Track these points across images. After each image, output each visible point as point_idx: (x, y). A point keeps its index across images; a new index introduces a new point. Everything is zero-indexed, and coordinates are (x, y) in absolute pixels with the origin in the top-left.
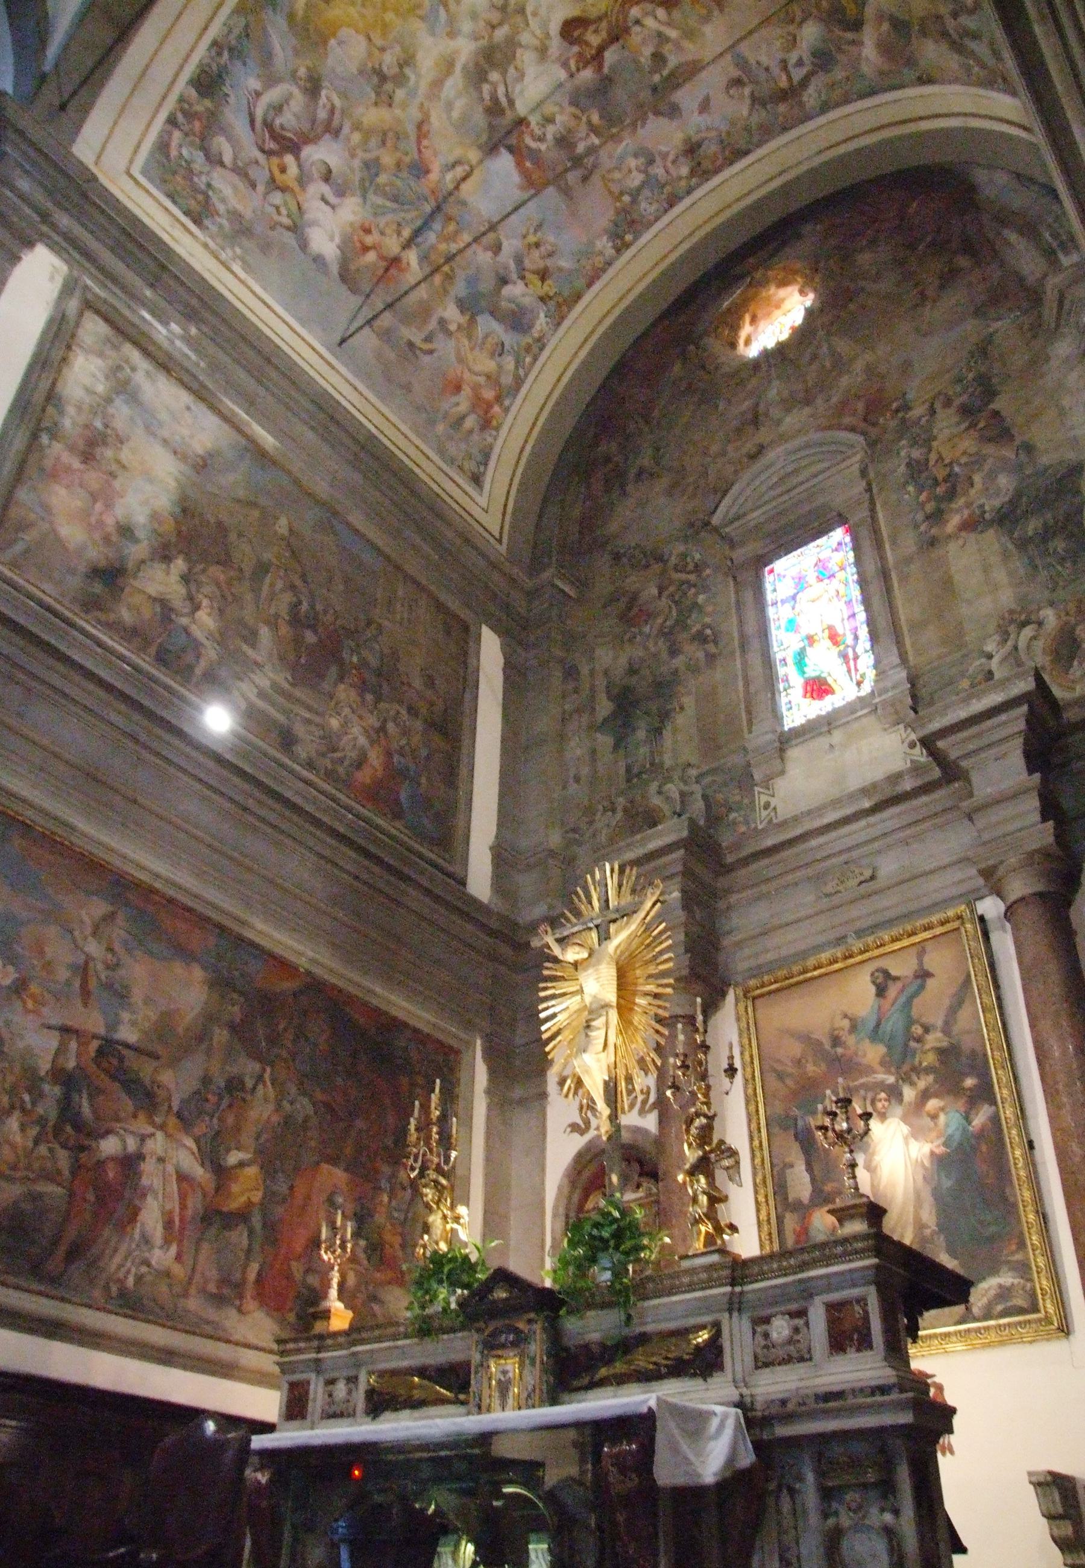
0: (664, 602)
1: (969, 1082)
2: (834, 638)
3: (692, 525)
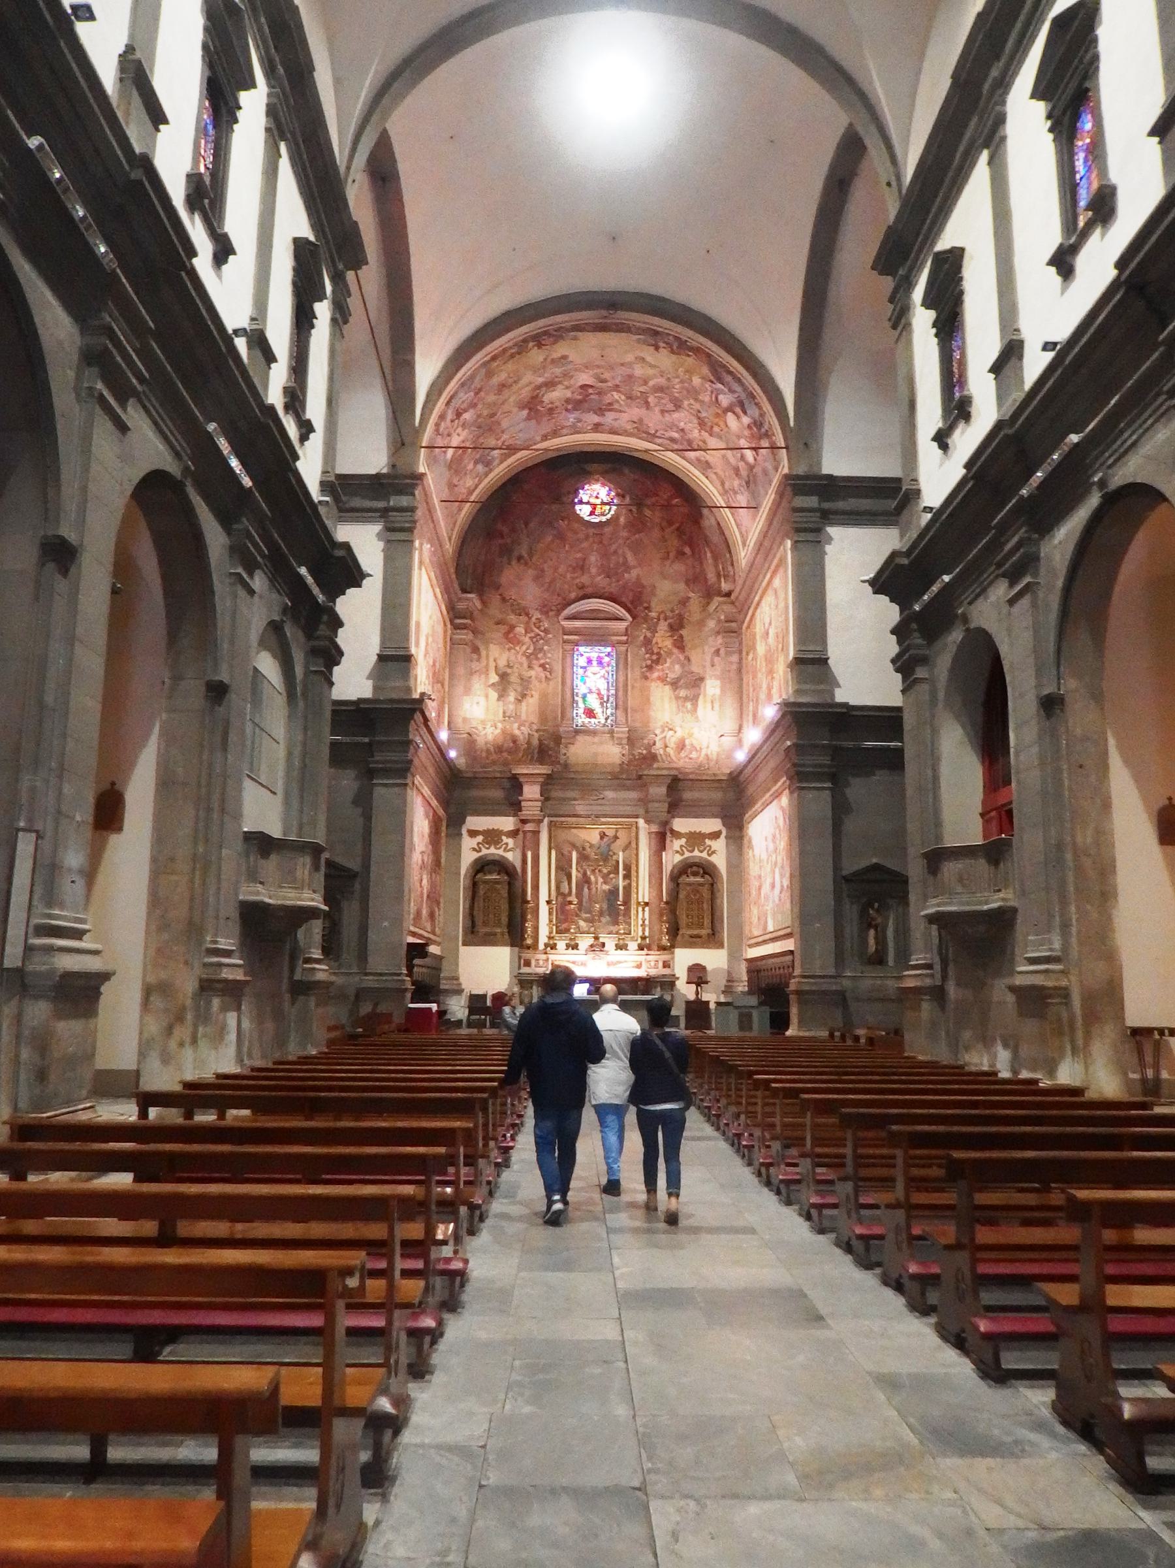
0: (527, 639)
2: (599, 694)
3: (545, 606)
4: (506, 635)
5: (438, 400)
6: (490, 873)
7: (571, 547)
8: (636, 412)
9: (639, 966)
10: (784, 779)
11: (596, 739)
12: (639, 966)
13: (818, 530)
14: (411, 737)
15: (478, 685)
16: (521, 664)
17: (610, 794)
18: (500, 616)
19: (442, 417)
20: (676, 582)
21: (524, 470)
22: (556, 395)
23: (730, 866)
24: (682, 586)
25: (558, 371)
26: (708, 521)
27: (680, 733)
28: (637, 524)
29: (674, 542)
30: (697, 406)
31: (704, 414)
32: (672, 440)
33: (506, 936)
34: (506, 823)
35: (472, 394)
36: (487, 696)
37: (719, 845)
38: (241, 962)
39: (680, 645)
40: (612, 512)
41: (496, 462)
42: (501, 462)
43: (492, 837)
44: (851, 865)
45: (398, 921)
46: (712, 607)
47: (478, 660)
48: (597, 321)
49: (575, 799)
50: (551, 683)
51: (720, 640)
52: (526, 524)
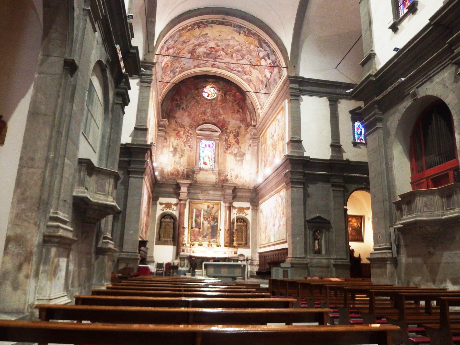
0: (184, 136)
1: (216, 220)
2: (209, 158)
3: (191, 125)
4: (177, 134)
5: (162, 39)
6: (167, 218)
7: (201, 106)
8: (228, 60)
9: (225, 253)
10: (284, 184)
11: (207, 173)
12: (225, 253)
13: (299, 96)
14: (146, 159)
15: (166, 151)
16: (182, 145)
17: (211, 192)
18: (175, 128)
19: (162, 47)
20: (237, 120)
21: (186, 79)
22: (201, 50)
23: (253, 219)
24: (238, 122)
25: (203, 40)
26: (248, 101)
27: (236, 172)
28: (224, 100)
29: (236, 108)
30: (251, 57)
31: (253, 61)
32: (239, 71)
33: (172, 242)
34: (174, 201)
35: (173, 42)
36: (169, 155)
37: (249, 212)
38: (71, 229)
39: (237, 142)
40: (215, 96)
41: (177, 73)
42: (179, 74)
43: (168, 205)
44: (310, 216)
45: (137, 231)
46: (249, 130)
47: (166, 142)
48: (220, 20)
49: (199, 193)
50: (192, 152)
51: (251, 141)
52: (186, 97)
